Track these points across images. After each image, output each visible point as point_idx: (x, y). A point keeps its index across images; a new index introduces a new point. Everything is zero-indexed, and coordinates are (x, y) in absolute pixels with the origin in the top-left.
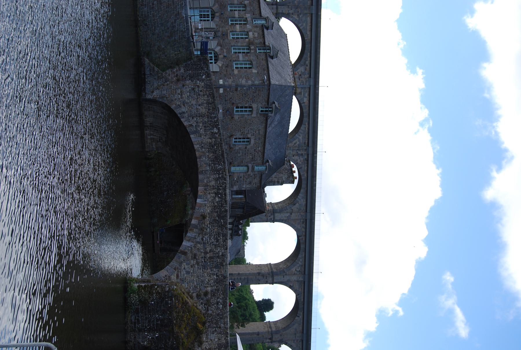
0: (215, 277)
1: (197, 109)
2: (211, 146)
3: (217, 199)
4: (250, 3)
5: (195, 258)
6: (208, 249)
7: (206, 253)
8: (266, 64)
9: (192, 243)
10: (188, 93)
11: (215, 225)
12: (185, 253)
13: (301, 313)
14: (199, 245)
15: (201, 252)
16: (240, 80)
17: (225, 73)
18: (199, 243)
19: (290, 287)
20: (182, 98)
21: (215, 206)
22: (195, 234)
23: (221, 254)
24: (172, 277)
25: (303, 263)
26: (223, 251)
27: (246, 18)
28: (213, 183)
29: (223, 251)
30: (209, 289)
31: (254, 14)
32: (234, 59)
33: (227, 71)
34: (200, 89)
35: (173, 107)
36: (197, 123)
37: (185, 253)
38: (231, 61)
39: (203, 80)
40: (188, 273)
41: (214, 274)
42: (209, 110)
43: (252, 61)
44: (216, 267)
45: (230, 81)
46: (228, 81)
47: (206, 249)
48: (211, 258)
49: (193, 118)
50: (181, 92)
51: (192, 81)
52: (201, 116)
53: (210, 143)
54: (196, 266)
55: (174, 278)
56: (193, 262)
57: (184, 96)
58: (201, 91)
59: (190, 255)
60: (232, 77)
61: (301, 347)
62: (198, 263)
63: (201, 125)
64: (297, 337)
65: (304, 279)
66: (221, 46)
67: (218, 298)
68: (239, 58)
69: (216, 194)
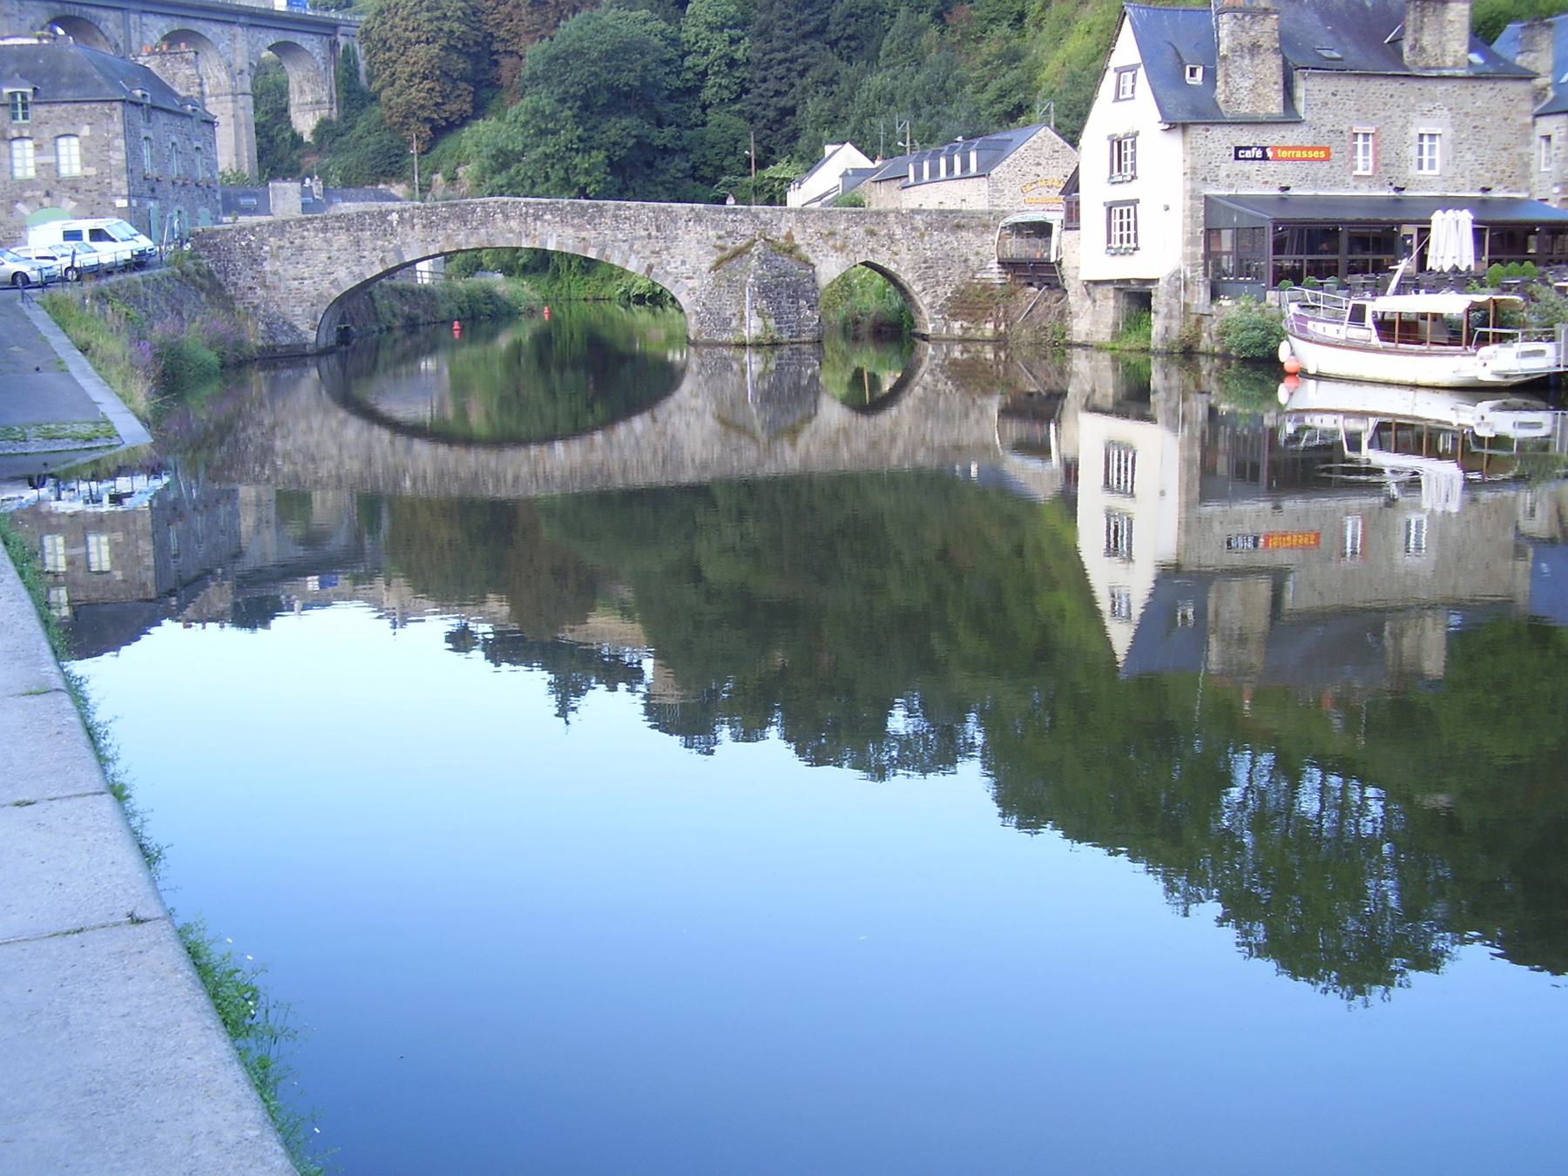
0: (691, 224)
1: (339, 250)
2: (429, 225)
3: (548, 217)
5: (658, 253)
7: (649, 236)
8: (64, 106)
9: (633, 256)
10: (299, 266)
11: (597, 221)
12: (650, 268)
14: (635, 247)
15: (648, 243)
16: (113, 162)
17: (95, 195)
18: (631, 247)
20: (312, 278)
21: (562, 221)
22: (616, 252)
23: (651, 214)
24: (690, 286)
26: (646, 211)
28: (513, 224)
29: (646, 211)
30: (711, 233)
33: (90, 191)
34: (288, 245)
35: (336, 294)
36: (374, 249)
37: (650, 268)
38: (58, 182)
39: (263, 242)
40: (683, 263)
41: (687, 226)
42: (341, 228)
43: (56, 135)
44: (674, 221)
45: (116, 183)
46: (119, 189)
47: (641, 237)
48: (658, 229)
49: (364, 257)
50: (294, 279)
51: (266, 259)
53: (424, 227)
54: (672, 251)
55: (691, 283)
56: (665, 255)
57: (306, 275)
58: (292, 243)
59: (653, 260)
60: (107, 181)
62: (668, 249)
63: (380, 243)
64: (14, 12)
67: (726, 220)
68: (49, 165)
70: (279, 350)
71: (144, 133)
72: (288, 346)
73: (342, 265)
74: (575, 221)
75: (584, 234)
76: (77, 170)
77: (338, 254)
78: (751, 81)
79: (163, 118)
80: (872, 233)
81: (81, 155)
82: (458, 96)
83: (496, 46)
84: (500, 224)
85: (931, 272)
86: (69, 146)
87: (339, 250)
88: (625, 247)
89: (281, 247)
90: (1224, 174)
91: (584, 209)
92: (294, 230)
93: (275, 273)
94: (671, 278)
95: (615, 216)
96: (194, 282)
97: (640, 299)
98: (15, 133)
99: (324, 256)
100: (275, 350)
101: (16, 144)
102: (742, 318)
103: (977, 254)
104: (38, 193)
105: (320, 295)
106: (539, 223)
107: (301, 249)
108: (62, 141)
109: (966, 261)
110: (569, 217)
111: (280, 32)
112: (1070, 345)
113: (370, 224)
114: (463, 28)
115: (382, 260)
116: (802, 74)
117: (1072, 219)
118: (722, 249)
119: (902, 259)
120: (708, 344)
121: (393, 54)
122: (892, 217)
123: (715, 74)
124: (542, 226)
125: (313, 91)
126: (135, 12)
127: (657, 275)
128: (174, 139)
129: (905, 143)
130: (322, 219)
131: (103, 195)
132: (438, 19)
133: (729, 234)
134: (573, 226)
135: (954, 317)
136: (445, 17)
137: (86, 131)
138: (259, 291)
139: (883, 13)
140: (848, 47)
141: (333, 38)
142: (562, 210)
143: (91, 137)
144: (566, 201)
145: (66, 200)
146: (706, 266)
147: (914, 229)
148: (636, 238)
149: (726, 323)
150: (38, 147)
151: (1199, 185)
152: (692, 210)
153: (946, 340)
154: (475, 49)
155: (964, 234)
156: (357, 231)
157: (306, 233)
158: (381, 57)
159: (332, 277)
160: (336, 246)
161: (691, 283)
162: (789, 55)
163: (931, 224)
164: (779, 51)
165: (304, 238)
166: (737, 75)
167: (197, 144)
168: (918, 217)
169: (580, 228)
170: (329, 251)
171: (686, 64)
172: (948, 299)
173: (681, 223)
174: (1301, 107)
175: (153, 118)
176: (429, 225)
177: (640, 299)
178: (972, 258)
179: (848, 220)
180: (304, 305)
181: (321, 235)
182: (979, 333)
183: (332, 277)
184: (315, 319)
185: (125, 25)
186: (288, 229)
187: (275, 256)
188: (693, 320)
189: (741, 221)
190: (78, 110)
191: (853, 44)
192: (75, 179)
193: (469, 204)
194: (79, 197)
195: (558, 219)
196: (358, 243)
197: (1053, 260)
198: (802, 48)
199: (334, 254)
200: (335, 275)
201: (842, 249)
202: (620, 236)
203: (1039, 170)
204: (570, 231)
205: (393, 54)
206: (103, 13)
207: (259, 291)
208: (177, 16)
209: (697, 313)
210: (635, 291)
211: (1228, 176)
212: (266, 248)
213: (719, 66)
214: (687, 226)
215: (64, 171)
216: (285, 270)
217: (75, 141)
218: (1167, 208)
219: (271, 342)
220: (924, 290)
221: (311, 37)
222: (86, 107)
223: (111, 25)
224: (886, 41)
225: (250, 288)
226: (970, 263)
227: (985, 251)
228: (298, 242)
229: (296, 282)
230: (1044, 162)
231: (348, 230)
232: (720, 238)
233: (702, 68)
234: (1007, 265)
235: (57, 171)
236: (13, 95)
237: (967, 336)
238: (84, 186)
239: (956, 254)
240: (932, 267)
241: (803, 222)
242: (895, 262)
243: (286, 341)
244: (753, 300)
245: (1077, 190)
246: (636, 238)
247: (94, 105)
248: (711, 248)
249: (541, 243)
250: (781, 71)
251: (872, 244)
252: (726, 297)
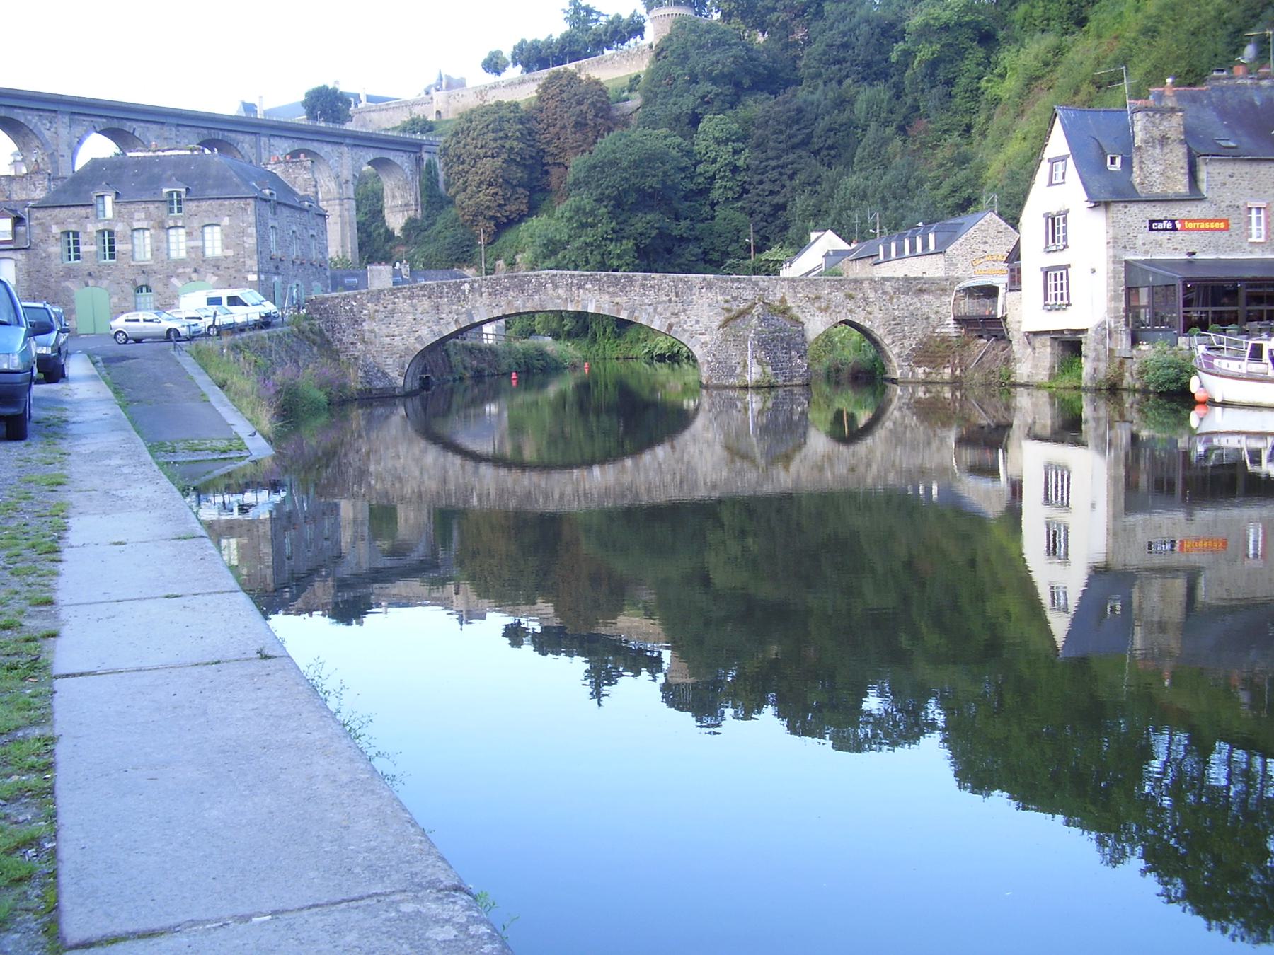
0: (703, 291)
1: (422, 313)
2: (494, 293)
3: (588, 286)
4: (57, 223)
6: (665, 299)
8: (209, 202)
11: (628, 289)
12: (671, 326)
13: (129, 123)
16: (247, 246)
18: (655, 310)
19: (80, 142)
23: (671, 283)
25: (35, 113)
27: (98, 231)
28: (561, 292)
30: (720, 298)
31: (87, 218)
32: (201, 254)
34: (382, 309)
35: (420, 348)
37: (671, 326)
38: (204, 261)
39: (362, 307)
40: (697, 322)
41: (700, 293)
42: (424, 296)
45: (249, 262)
46: (251, 266)
48: (677, 295)
52: (437, 307)
53: (490, 294)
55: (703, 338)
56: (682, 316)
57: (396, 333)
59: (673, 320)
61: (188, 129)
62: (685, 311)
63: (455, 307)
65: (65, 113)
66: (170, 277)
68: (197, 247)
69: (580, 286)
70: (374, 392)
71: (271, 223)
72: (381, 389)
73: (424, 325)
74: (611, 289)
75: (617, 300)
76: (218, 252)
77: (421, 316)
78: (750, 183)
79: (286, 212)
80: (850, 297)
81: (222, 240)
82: (517, 199)
83: (547, 159)
84: (550, 292)
85: (899, 327)
86: (213, 233)
87: (422, 313)
88: (651, 310)
89: (377, 311)
90: (1141, 243)
91: (618, 280)
92: (388, 298)
93: (372, 331)
94: (688, 334)
95: (643, 285)
96: (308, 338)
97: (661, 358)
98: (171, 223)
99: (410, 318)
100: (371, 392)
101: (172, 232)
102: (745, 366)
103: (937, 312)
104: (188, 270)
105: (407, 349)
106: (581, 291)
107: (393, 312)
108: (207, 230)
109: (927, 318)
110: (605, 285)
111: (377, 150)
112: (1015, 385)
113: (447, 293)
114: (521, 145)
115: (457, 321)
116: (791, 177)
117: (1015, 282)
118: (729, 310)
119: (875, 317)
120: (718, 387)
121: (466, 167)
122: (866, 284)
123: (722, 178)
124: (584, 293)
125: (402, 196)
126: (265, 135)
127: (676, 332)
128: (294, 228)
129: (875, 230)
130: (409, 289)
131: (238, 271)
132: (501, 138)
133: (735, 299)
134: (608, 293)
135: (918, 364)
136: (507, 137)
137: (226, 221)
138: (359, 346)
139: (856, 127)
140: (829, 155)
141: (418, 155)
142: (600, 280)
143: (230, 226)
144: (603, 273)
145: (209, 275)
146: (715, 325)
147: (884, 293)
148: (659, 303)
149: (732, 370)
150: (189, 234)
151: (1120, 252)
152: (705, 279)
153: (911, 382)
154: (530, 162)
155: (925, 296)
156: (437, 297)
157: (396, 300)
158: (456, 169)
159: (417, 335)
160: (420, 310)
161: (703, 338)
162: (780, 163)
163: (898, 289)
164: (773, 159)
165: (395, 303)
166: (739, 178)
167: (312, 232)
168: (888, 284)
169: (614, 294)
170: (415, 314)
171: (698, 170)
172: (913, 350)
173: (696, 290)
174: (1203, 187)
175: (278, 211)
176: (494, 293)
177: (661, 358)
178: (933, 316)
179: (830, 287)
180: (394, 357)
181: (408, 301)
182: (939, 377)
183: (417, 335)
184: (403, 368)
185: (257, 146)
186: (382, 296)
187: (372, 318)
188: (705, 368)
189: (744, 288)
190: (220, 205)
191: (833, 153)
192: (217, 259)
193: (526, 276)
194: (220, 272)
195: (596, 288)
196: (437, 307)
197: (999, 316)
198: (792, 157)
199: (419, 316)
200: (419, 333)
201: (826, 310)
202: (646, 301)
203: (986, 247)
204: (607, 297)
205: (466, 167)
206: (240, 137)
207: (359, 346)
208: (297, 138)
209: (709, 362)
210: (657, 352)
211: (1144, 244)
212: (365, 312)
213: (724, 171)
214: (700, 293)
215: (209, 253)
216: (380, 329)
217: (217, 229)
218: (1094, 271)
219: (368, 386)
220: (893, 342)
221: (402, 154)
222: (227, 202)
223: (246, 146)
224: (859, 150)
225: (352, 343)
226: (931, 320)
227: (943, 310)
228: (390, 307)
229: (388, 339)
230: (990, 241)
231: (430, 297)
232: (727, 301)
233: (711, 174)
234: (961, 321)
235: (203, 252)
236: (171, 194)
237: (929, 379)
238: (224, 264)
239: (919, 313)
240: (899, 324)
241: (794, 288)
242: (870, 320)
243: (380, 385)
244: (754, 351)
245: (1019, 259)
246: (659, 303)
247: (232, 201)
248: (720, 310)
249: (583, 306)
250: (774, 175)
251: (851, 305)
252: (732, 349)
